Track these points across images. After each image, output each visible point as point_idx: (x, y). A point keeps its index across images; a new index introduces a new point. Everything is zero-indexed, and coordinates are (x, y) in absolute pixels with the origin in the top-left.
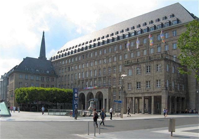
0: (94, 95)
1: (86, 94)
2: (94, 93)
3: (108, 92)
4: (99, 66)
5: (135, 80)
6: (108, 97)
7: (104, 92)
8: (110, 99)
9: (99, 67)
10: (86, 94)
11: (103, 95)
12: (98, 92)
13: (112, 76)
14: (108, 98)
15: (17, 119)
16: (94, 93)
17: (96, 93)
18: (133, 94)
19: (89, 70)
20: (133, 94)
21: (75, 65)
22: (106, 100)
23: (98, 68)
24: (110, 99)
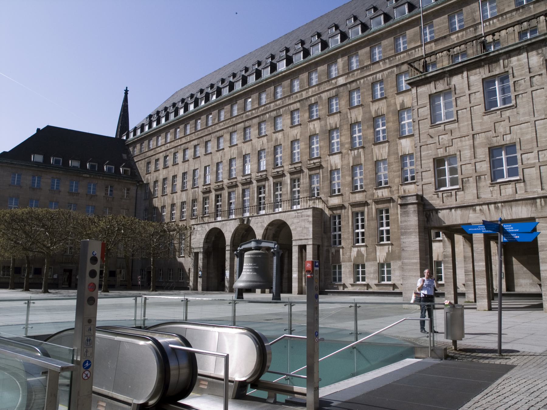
0: (259, 233)
1: (229, 229)
2: (259, 227)
3: (311, 219)
4: (274, 136)
5: (480, 139)
6: (311, 237)
7: (296, 221)
8: (319, 246)
9: (274, 139)
10: (229, 229)
11: (293, 232)
12: (270, 225)
13: (322, 164)
14: (311, 242)
15: (38, 305)
16: (259, 227)
17: (265, 226)
18: (472, 206)
19: (240, 153)
20: (472, 206)
21: (195, 142)
22: (302, 248)
23: (273, 144)
24: (319, 246)
